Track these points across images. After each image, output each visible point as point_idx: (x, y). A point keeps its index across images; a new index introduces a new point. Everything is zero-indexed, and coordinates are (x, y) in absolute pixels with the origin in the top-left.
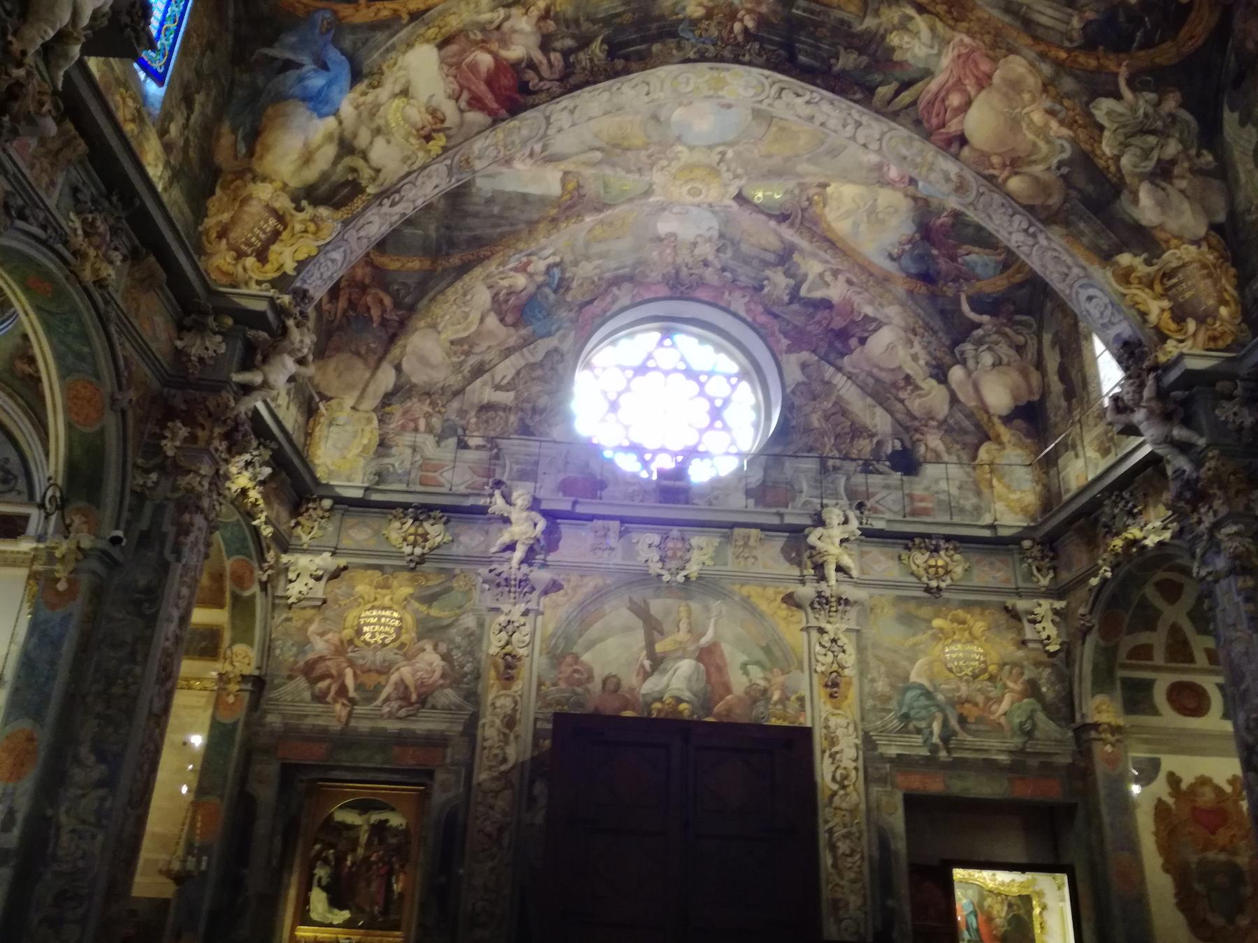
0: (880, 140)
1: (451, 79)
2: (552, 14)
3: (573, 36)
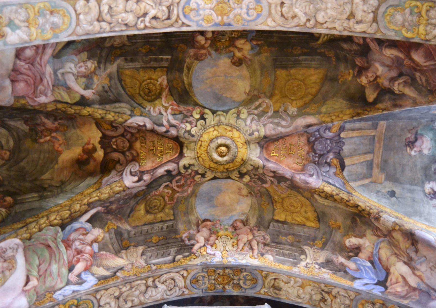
0: (78, 15)
2: (357, 69)
3: (342, 49)
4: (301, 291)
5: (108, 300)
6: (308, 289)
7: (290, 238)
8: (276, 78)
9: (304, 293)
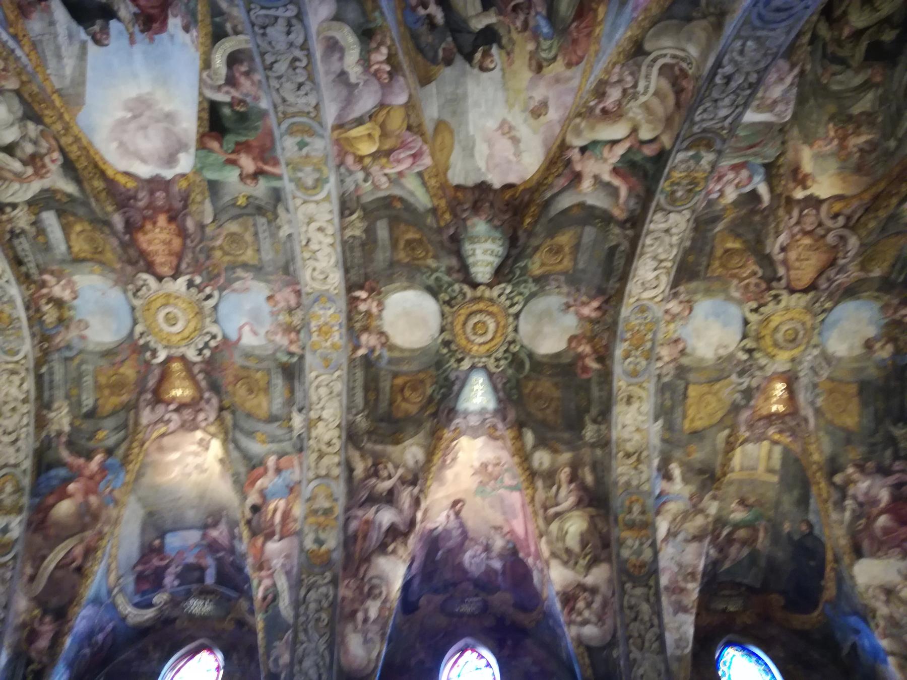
1: (890, 551)
3: (885, 449)
4: (634, 429)
5: (670, 221)
6: (637, 437)
7: (668, 403)
8: (848, 383)
9: (631, 433)
